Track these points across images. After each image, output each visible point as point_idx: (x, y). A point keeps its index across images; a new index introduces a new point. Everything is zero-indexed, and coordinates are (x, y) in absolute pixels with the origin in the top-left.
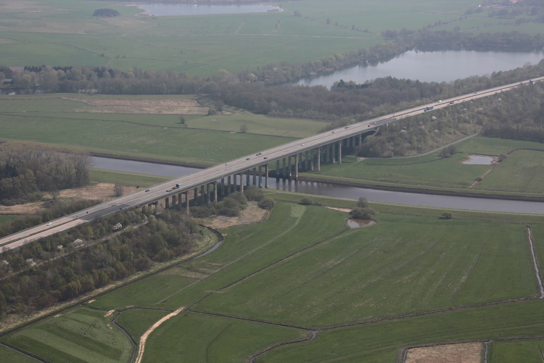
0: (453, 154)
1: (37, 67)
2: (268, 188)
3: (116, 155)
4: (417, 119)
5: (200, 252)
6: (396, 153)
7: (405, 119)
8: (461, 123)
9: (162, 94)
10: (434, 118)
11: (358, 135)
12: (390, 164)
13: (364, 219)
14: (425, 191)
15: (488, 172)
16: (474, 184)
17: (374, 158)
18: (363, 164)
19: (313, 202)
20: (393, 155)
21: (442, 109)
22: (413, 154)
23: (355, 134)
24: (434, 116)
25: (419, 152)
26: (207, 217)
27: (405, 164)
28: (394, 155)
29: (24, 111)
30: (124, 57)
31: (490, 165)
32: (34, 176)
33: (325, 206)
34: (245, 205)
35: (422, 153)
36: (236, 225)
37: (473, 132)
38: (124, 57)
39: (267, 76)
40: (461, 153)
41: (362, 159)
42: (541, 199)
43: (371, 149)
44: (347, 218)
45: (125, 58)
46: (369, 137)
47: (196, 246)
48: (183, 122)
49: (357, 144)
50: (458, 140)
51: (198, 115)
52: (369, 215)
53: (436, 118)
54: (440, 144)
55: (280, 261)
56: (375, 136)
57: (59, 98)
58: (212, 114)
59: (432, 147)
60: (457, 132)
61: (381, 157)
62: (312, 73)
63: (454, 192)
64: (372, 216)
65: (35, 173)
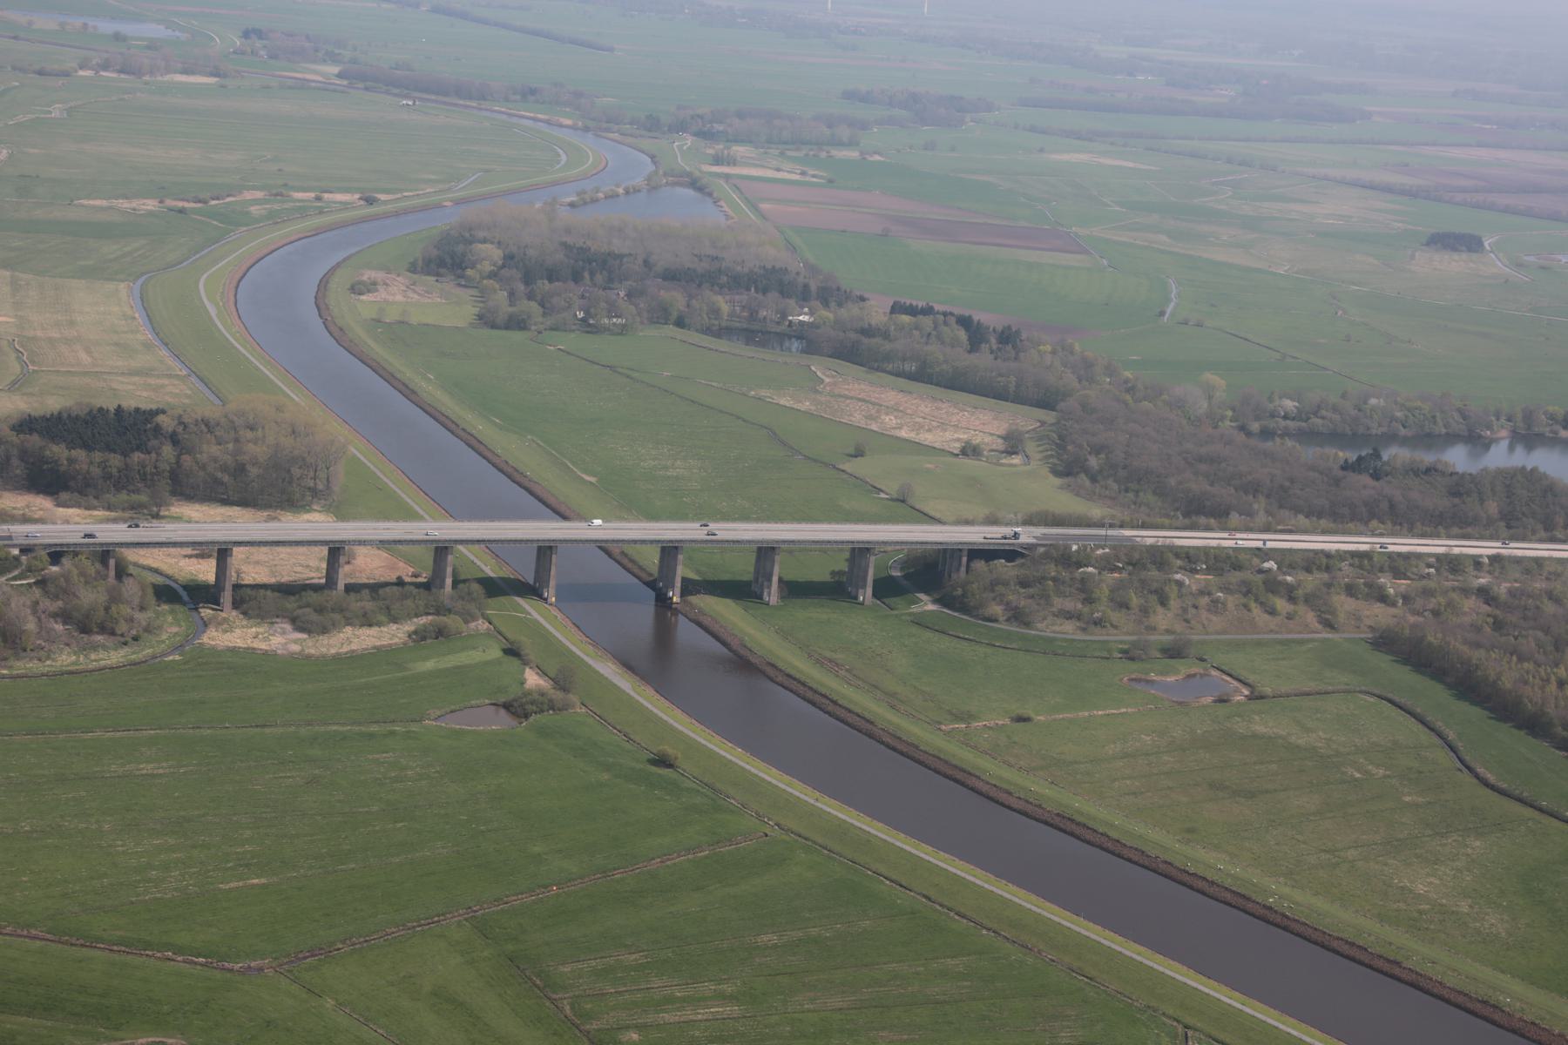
0: (1183, 658)
1: (917, 306)
2: (551, 604)
3: (525, 477)
4: (1190, 558)
5: (19, 672)
6: (1017, 616)
7: (1152, 546)
8: (1357, 599)
9: (1007, 401)
10: (1271, 565)
11: (960, 550)
12: (962, 635)
13: (513, 714)
14: (828, 702)
15: (1115, 711)
16: (984, 723)
17: (956, 614)
18: (908, 618)
19: (522, 653)
20: (1001, 619)
21: (1333, 552)
22: (1068, 628)
23: (946, 543)
24: (1273, 563)
25: (1084, 630)
26: (262, 619)
27: (997, 644)
28: (1007, 620)
29: (665, 373)
30: (1199, 325)
31: (1177, 702)
32: (170, 464)
33: (531, 668)
34: (383, 618)
35: (1092, 634)
36: (254, 649)
37: (1370, 627)
38: (1199, 325)
39: (1324, 413)
40: (1202, 660)
41: (931, 607)
42: (1005, 795)
43: (959, 592)
44: (487, 701)
45: (1202, 326)
46: (979, 565)
47: (40, 660)
48: (859, 453)
49: (958, 570)
50: (1277, 633)
51: (943, 450)
52: (530, 707)
53: (1275, 567)
54: (1192, 628)
55: (82, 732)
56: (1013, 566)
57: (809, 366)
58: (968, 455)
59: (1152, 629)
60: (1311, 617)
61: (972, 617)
62: (1488, 433)
63: (872, 723)
64: (551, 712)
65: (178, 457)
